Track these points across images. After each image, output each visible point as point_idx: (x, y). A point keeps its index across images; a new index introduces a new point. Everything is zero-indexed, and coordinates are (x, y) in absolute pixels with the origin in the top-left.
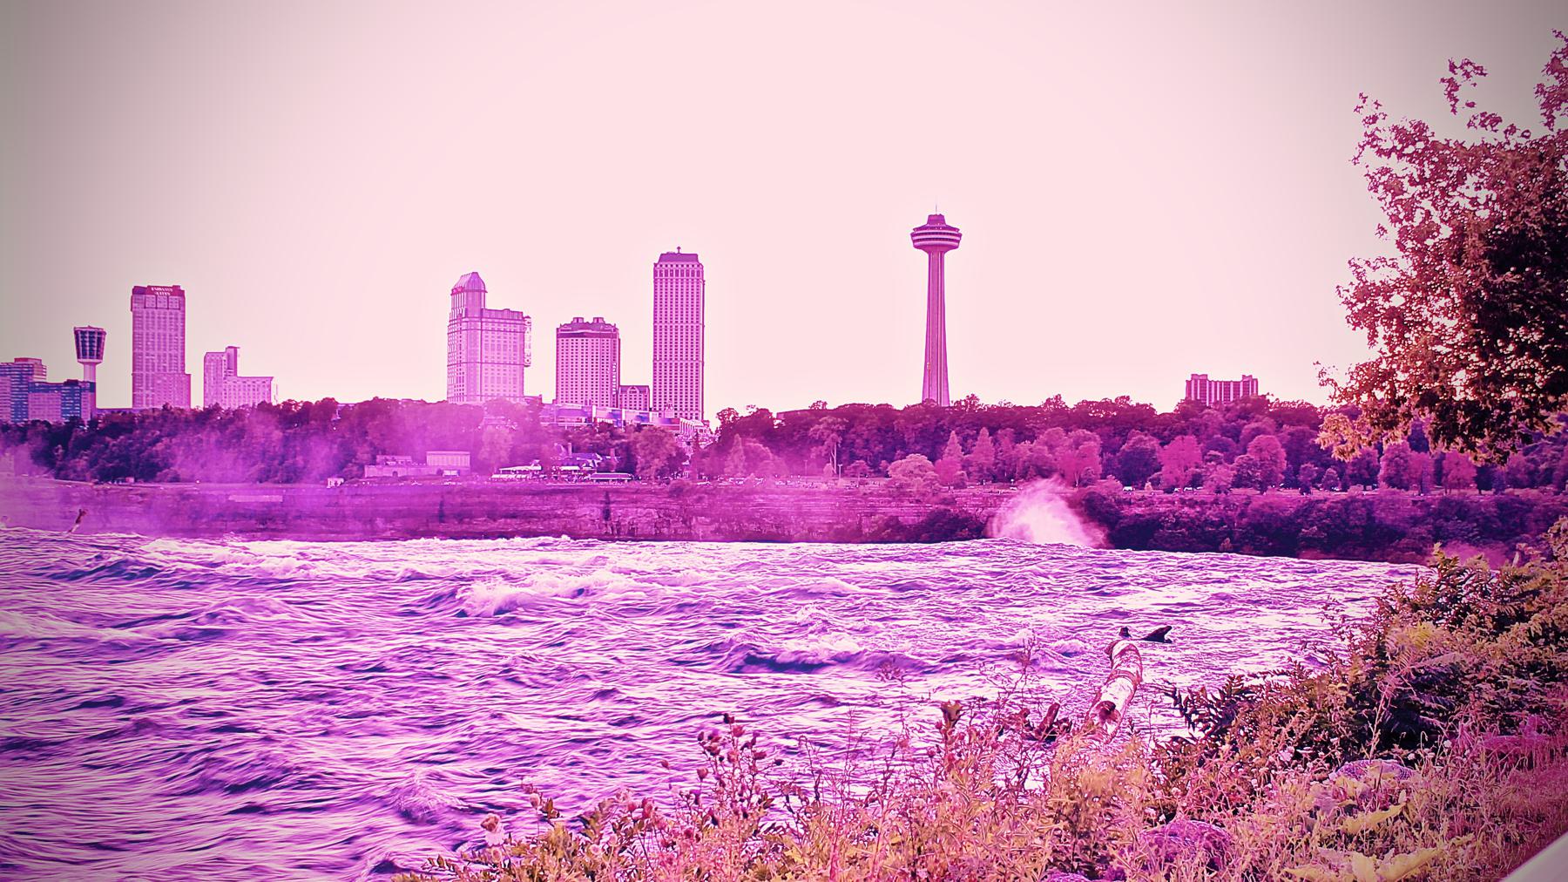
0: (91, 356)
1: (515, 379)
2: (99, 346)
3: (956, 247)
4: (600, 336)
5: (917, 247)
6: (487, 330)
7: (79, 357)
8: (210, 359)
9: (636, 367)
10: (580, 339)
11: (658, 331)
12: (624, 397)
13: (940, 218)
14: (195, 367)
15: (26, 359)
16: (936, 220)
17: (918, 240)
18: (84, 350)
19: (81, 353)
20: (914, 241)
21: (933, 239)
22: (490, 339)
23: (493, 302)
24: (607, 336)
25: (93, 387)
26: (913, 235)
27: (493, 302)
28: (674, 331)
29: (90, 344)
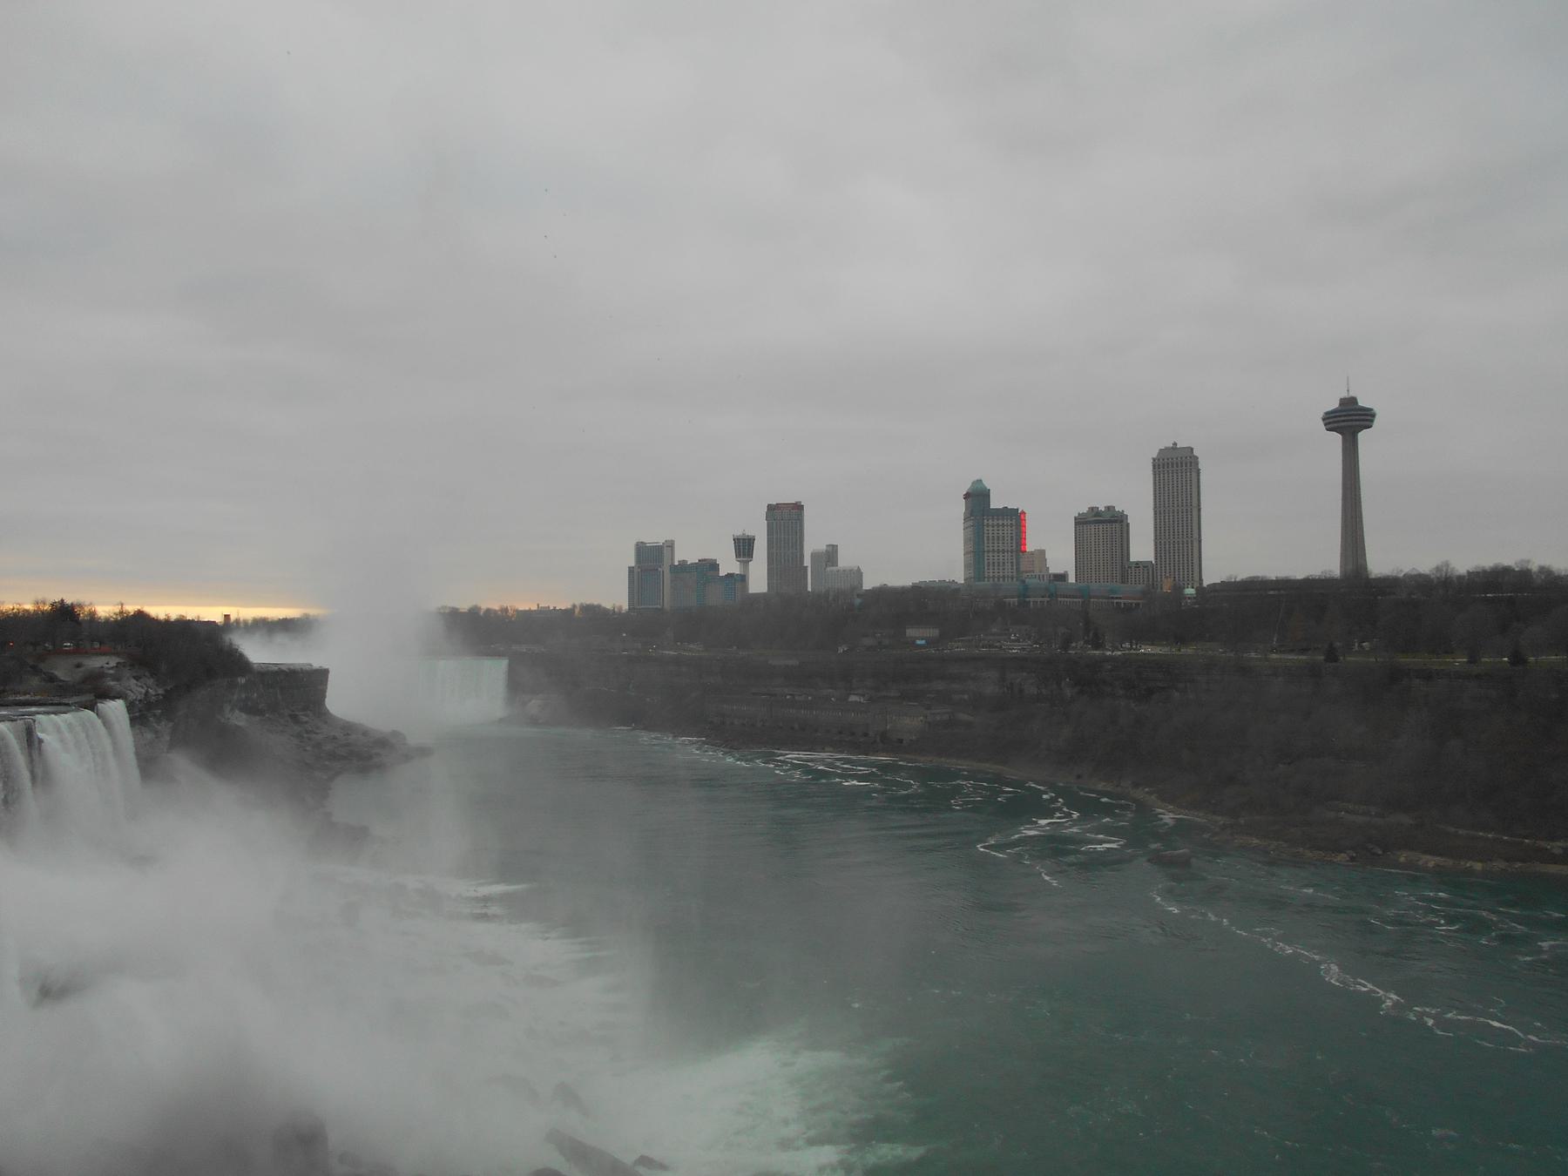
0: (744, 555)
1: (1012, 563)
2: (739, 549)
3: (1370, 427)
4: (1110, 522)
5: (1328, 430)
6: (988, 525)
7: (736, 557)
8: (814, 556)
9: (1142, 548)
10: (1093, 526)
11: (1158, 515)
12: (1129, 572)
13: (1353, 400)
14: (807, 562)
15: (705, 560)
16: (1349, 404)
17: (1330, 423)
18: (740, 552)
19: (738, 555)
20: (1325, 425)
21: (1356, 420)
22: (991, 532)
23: (995, 503)
24: (1116, 521)
25: (743, 579)
26: (1324, 420)
27: (995, 503)
28: (1171, 514)
29: (744, 547)
